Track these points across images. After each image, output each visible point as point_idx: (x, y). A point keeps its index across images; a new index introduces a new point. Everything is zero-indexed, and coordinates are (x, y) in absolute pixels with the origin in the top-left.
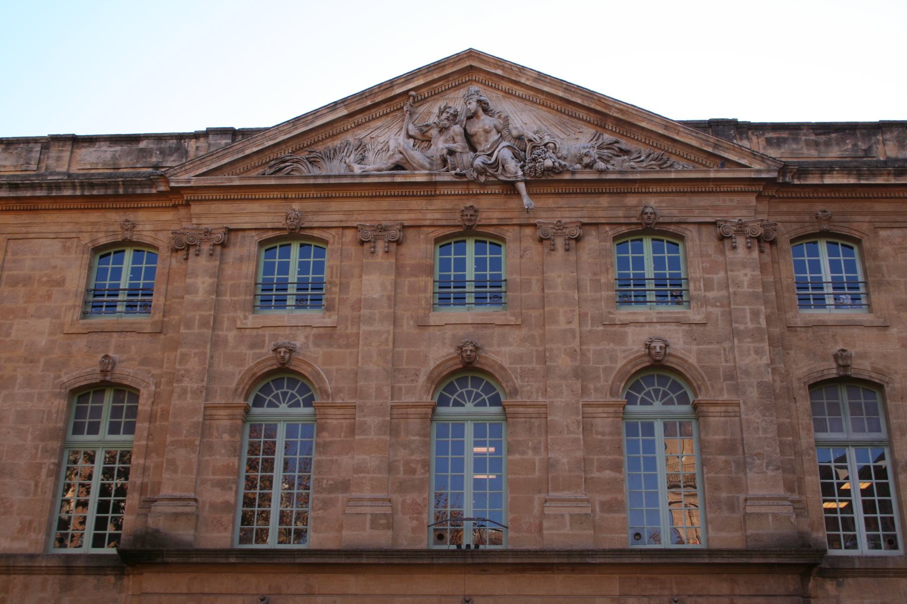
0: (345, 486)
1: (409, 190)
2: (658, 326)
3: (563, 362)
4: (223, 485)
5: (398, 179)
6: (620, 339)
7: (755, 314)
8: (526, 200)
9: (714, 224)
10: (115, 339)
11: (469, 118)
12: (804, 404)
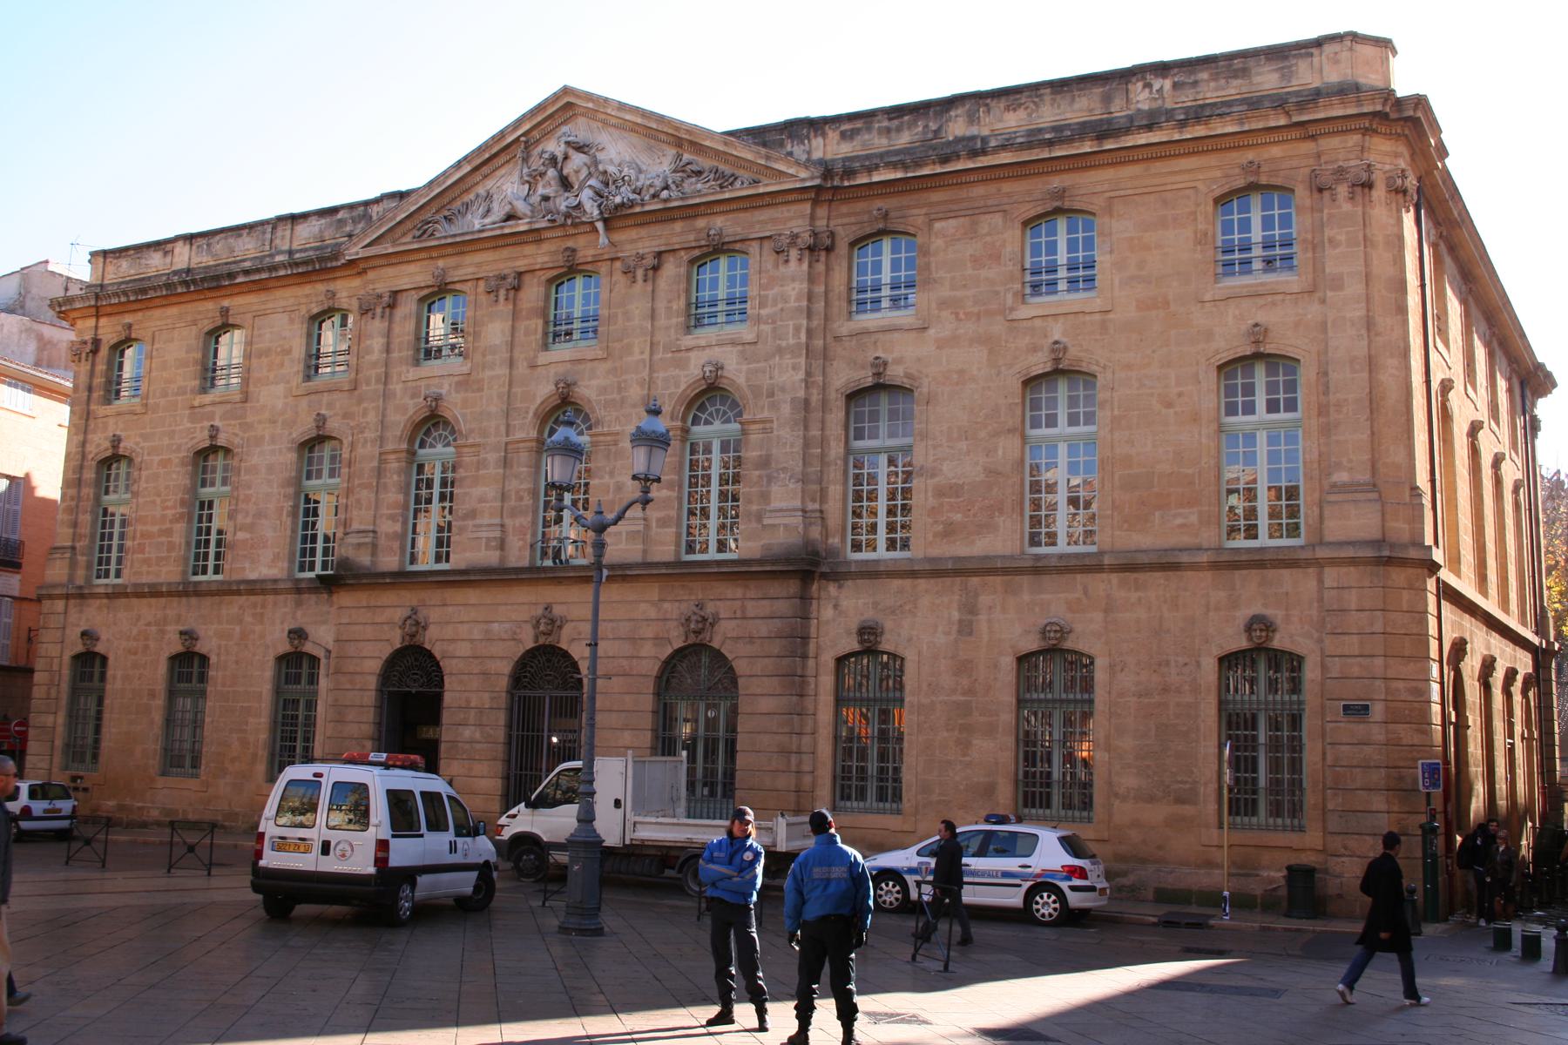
1: (517, 239)
2: (716, 348)
4: (392, 518)
6: (682, 364)
7: (797, 329)
9: (770, 237)
10: (326, 398)
12: (837, 416)
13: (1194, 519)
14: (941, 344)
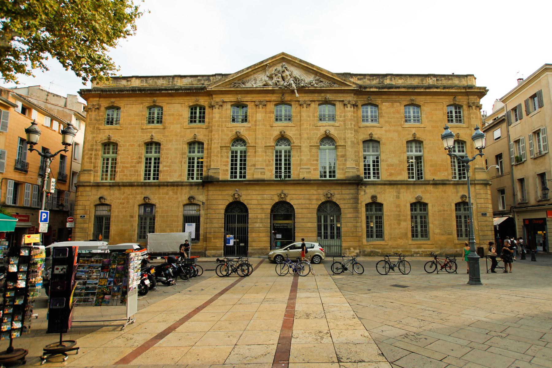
0: (254, 165)
3: (305, 136)
5: (265, 89)
7: (351, 124)
8: (297, 95)
10: (197, 130)
11: (283, 72)
12: (361, 145)
13: (446, 174)
14: (386, 131)
